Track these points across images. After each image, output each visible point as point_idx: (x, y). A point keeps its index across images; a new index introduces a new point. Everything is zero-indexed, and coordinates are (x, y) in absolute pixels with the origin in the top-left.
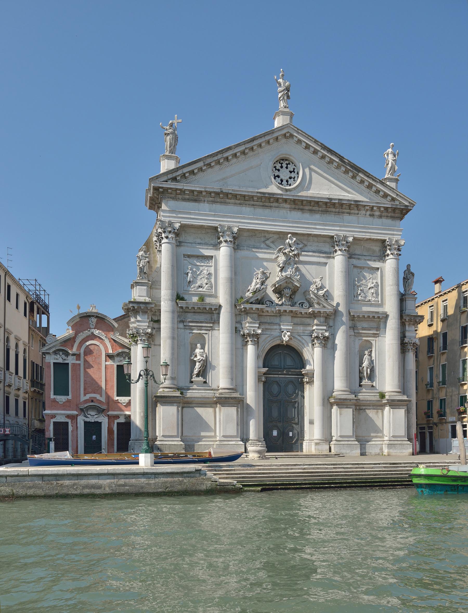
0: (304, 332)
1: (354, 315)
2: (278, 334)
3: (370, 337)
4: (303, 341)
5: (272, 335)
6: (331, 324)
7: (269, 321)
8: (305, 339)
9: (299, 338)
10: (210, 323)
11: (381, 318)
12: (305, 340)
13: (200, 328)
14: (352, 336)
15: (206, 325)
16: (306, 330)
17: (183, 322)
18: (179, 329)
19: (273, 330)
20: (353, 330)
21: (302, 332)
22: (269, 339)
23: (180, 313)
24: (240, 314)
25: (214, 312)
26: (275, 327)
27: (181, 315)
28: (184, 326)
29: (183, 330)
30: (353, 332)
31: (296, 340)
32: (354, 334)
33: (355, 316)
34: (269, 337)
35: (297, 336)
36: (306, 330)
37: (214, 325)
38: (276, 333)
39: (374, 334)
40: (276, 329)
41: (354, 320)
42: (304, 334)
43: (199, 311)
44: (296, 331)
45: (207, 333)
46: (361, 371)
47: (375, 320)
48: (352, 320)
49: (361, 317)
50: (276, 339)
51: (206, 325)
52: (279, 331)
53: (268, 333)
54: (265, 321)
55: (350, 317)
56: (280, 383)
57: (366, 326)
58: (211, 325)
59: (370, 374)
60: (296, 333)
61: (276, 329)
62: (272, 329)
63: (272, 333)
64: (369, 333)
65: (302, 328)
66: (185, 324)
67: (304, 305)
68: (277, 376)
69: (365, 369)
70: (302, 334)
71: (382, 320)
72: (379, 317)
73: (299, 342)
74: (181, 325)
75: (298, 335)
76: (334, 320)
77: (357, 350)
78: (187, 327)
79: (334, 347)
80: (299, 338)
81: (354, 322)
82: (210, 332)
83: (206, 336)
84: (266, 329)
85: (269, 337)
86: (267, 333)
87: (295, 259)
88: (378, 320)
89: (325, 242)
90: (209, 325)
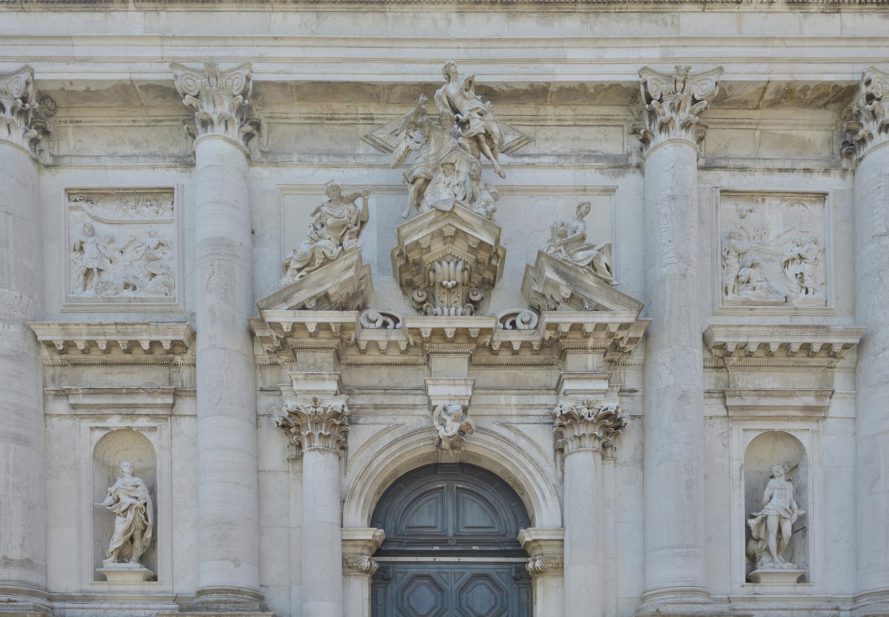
0: (525, 412)
1: (723, 346)
2: (424, 423)
3: (789, 419)
4: (522, 443)
5: (398, 425)
6: (631, 379)
7: (386, 382)
8: (529, 434)
9: (504, 432)
10: (164, 393)
11: (837, 349)
12: (528, 439)
13: (130, 411)
14: (718, 421)
15: (150, 400)
16: (531, 406)
17: (63, 394)
18: (55, 420)
19: (402, 412)
20: (720, 401)
21: (514, 412)
22: (387, 439)
23: (58, 369)
24: (277, 364)
25: (178, 359)
26: (411, 400)
27: (61, 376)
28: (74, 406)
29: (68, 422)
30: (721, 406)
31: (492, 440)
32: (724, 412)
33: (731, 348)
34: (388, 430)
35: (496, 428)
36: (531, 406)
37: (179, 402)
38: (415, 419)
39: (806, 408)
40: (415, 406)
41: (724, 367)
42: (525, 419)
43: (116, 355)
44: (494, 412)
45: (154, 429)
46: (754, 535)
47: (814, 361)
48: (717, 368)
49: (753, 348)
50: (418, 437)
51: (150, 400)
52: (426, 412)
53: (386, 421)
54: (374, 381)
55: (708, 355)
56: (441, 582)
57: (776, 385)
58: (169, 400)
59: (792, 540)
60: (494, 418)
61: (415, 406)
62: (399, 407)
63: (400, 420)
64: (786, 408)
65: (514, 400)
66: (72, 401)
67: (519, 324)
68: (430, 559)
69: (773, 523)
70: (514, 420)
71: (839, 364)
72: (827, 347)
73: (504, 445)
74: (60, 407)
75: (502, 424)
76: (643, 368)
77: (736, 466)
78: (82, 412)
79: (643, 459)
80: (504, 432)
81: (723, 375)
82: (164, 427)
83: (152, 437)
84: (376, 407)
85: (388, 430)
86: (379, 419)
87: (479, 158)
88: (823, 360)
89: (605, 122)
90: (159, 401)
